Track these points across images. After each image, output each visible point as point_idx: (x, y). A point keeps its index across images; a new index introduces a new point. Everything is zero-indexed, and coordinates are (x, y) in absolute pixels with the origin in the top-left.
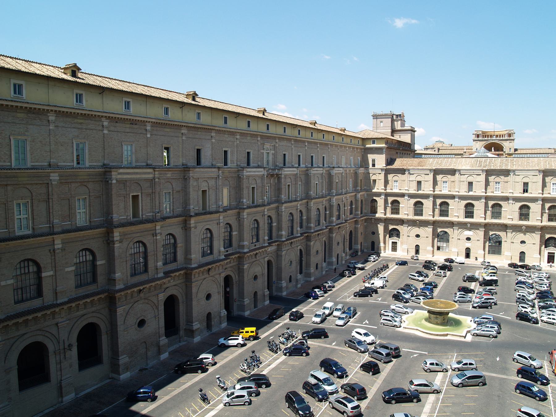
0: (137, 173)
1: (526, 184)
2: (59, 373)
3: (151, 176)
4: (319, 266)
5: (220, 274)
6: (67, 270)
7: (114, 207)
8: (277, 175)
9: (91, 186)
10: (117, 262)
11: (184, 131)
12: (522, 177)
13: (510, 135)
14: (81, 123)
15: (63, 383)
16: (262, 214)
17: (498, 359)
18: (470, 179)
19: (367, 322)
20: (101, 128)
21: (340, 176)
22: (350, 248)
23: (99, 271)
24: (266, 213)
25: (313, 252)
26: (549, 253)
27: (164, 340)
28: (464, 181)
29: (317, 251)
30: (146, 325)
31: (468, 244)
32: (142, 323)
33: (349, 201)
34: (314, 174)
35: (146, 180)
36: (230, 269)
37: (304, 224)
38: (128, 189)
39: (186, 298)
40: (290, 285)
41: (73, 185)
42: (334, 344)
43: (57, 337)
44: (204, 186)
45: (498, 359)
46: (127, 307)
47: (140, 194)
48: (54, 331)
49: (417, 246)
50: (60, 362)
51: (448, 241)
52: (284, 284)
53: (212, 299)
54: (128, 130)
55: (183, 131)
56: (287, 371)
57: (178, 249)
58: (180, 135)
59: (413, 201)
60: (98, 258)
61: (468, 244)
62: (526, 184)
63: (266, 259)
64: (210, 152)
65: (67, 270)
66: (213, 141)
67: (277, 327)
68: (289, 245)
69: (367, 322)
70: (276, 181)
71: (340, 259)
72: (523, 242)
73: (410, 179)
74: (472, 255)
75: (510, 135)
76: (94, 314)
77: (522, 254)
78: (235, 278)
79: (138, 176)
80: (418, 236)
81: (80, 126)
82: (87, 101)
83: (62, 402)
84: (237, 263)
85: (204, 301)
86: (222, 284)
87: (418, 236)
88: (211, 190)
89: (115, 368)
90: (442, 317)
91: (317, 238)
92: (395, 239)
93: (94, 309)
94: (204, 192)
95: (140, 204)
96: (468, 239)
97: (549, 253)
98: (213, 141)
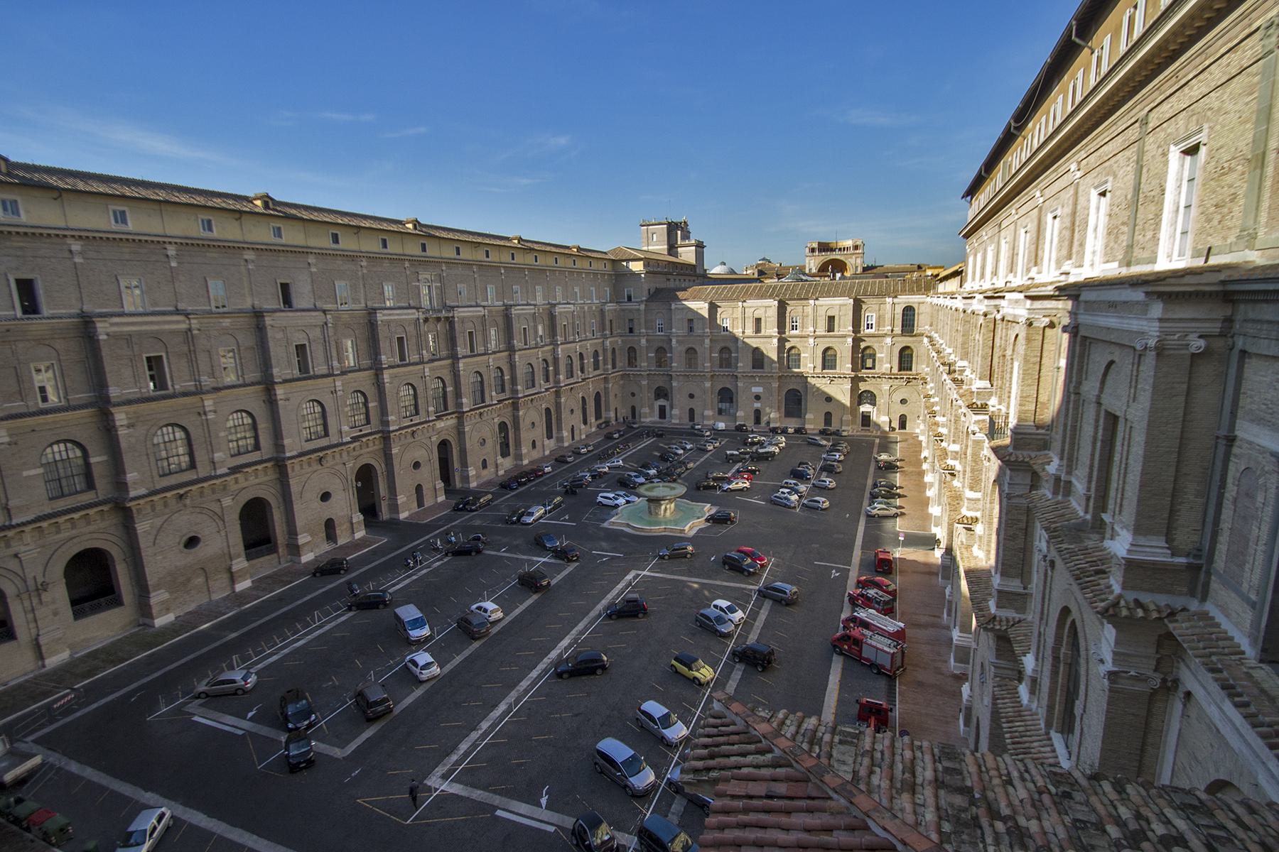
0: (152, 323)
2: (32, 625)
3: (184, 326)
6: (25, 474)
7: (108, 375)
8: (447, 318)
9: (59, 345)
10: (127, 459)
11: (249, 255)
14: (21, 248)
15: (42, 641)
20: (67, 254)
21: (570, 316)
22: (598, 416)
23: (97, 472)
25: (525, 425)
27: (240, 564)
30: (201, 544)
31: (757, 405)
32: (192, 542)
33: (591, 350)
34: (519, 316)
35: (173, 332)
37: (507, 387)
38: (136, 348)
39: (284, 500)
40: (485, 472)
41: (20, 345)
43: (20, 573)
44: (300, 339)
46: (158, 522)
47: (164, 355)
48: (13, 565)
50: (33, 610)
51: (731, 401)
52: (472, 472)
53: (333, 499)
54: (127, 257)
55: (246, 257)
57: (260, 432)
58: (243, 263)
59: (683, 348)
60: (90, 452)
61: (757, 405)
64: (309, 287)
65: (25, 474)
66: (314, 270)
71: (576, 432)
76: (97, 532)
78: (380, 467)
79: (155, 327)
81: (19, 253)
82: (27, 212)
83: (44, 666)
85: (317, 503)
88: (313, 344)
89: (144, 609)
92: (662, 402)
93: (92, 528)
94: (301, 349)
95: (167, 370)
96: (758, 397)
98: (314, 270)
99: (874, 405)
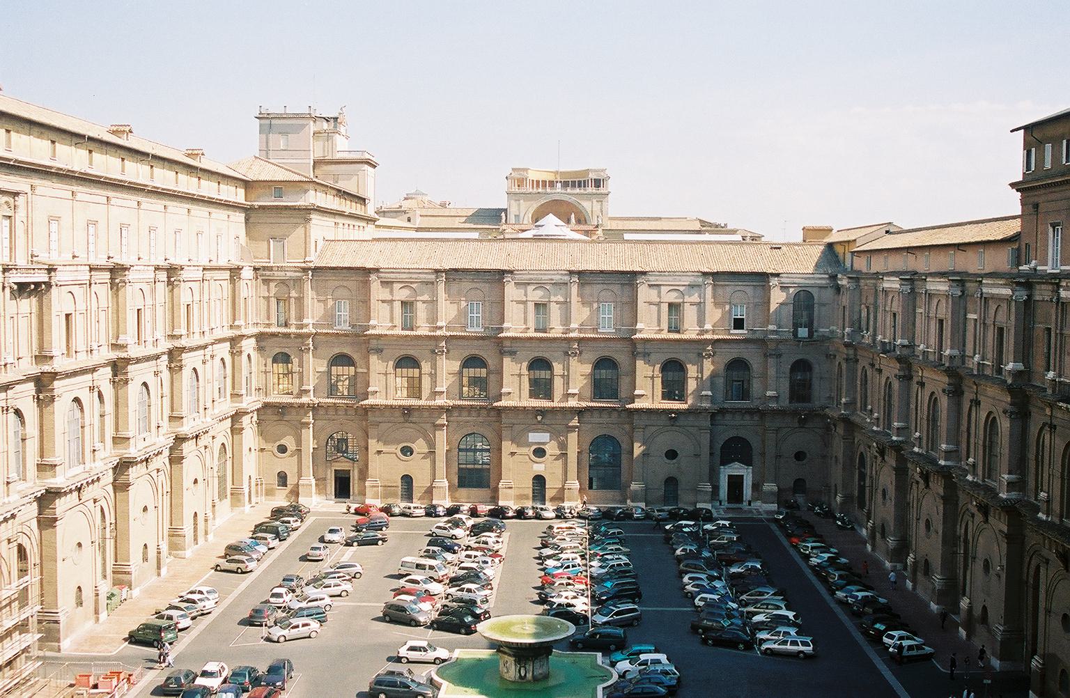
4: (152, 553)
13: (597, 183)
31: (539, 468)
68: (75, 494)
75: (597, 183)
99: (747, 462)
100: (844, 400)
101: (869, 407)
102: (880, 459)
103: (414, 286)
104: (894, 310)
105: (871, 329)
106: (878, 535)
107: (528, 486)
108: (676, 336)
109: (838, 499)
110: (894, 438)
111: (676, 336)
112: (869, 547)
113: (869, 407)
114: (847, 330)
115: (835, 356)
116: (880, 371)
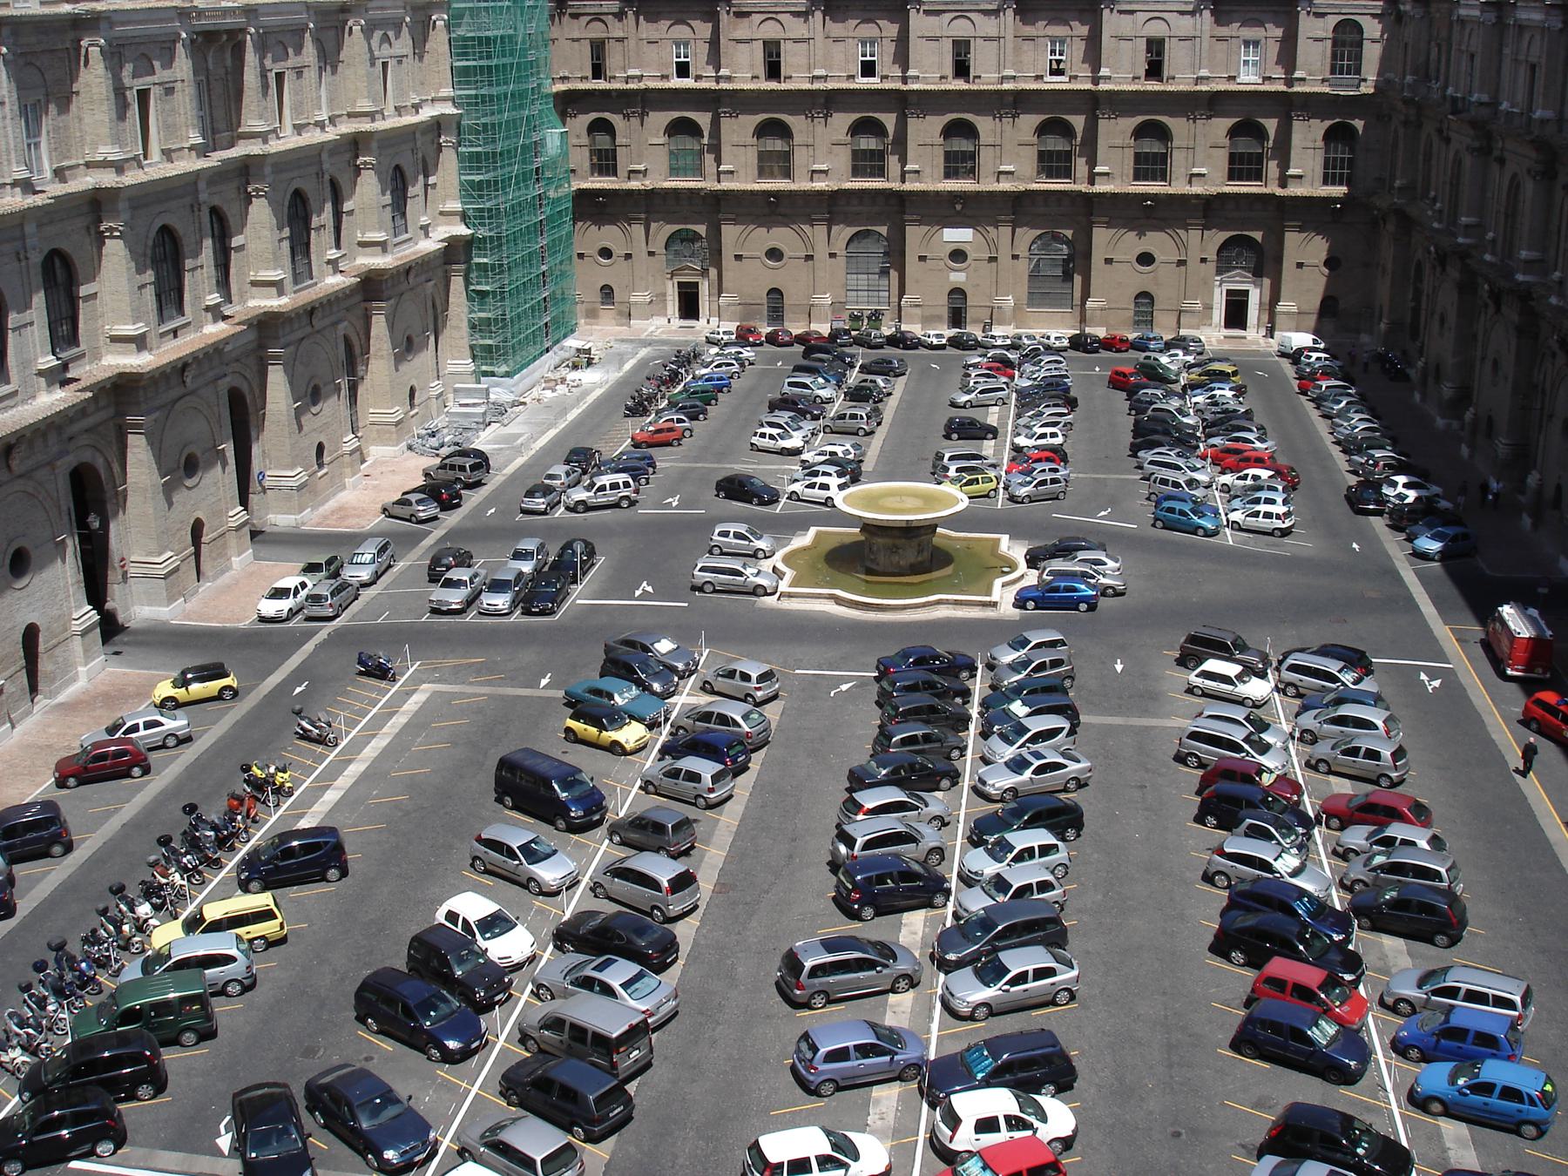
1: (1156, 47)
5: (50, 464)
12: (1142, 17)
16: (188, 200)
17: (1119, 667)
18: (961, 29)
19: (650, 589)
24: (203, 197)
26: (1229, 292)
28: (937, 39)
29: (409, 339)
31: (958, 278)
36: (85, 440)
42: (544, 682)
45: (1119, 667)
49: (775, 293)
56: (397, 806)
62: (1156, 47)
63: (224, 385)
67: (309, 647)
68: (305, 320)
69: (650, 589)
70: (229, 62)
72: (1146, 259)
73: (739, 35)
74: (971, 314)
77: (1145, 298)
80: (775, 254)
84: (111, 411)
86: (67, 502)
87: (775, 254)
90: (915, 542)
91: (404, 286)
96: (958, 255)
97: (1229, 292)
100: (1398, 183)
101: (1432, 194)
102: (1439, 269)
103: (779, 17)
104: (1473, 49)
105: (1442, 78)
106: (1431, 380)
107: (942, 307)
108: (1153, 86)
109: (1382, 326)
110: (1460, 240)
111: (1153, 86)
112: (1417, 397)
113: (1432, 194)
114: (1409, 78)
115: (1390, 119)
116: (1448, 140)
